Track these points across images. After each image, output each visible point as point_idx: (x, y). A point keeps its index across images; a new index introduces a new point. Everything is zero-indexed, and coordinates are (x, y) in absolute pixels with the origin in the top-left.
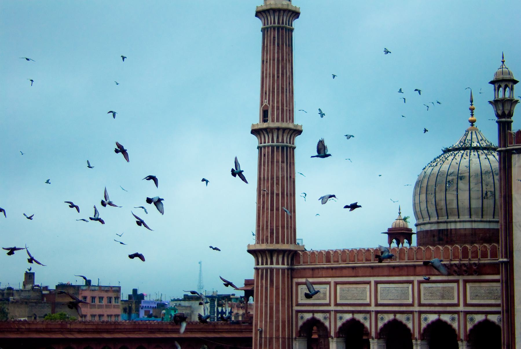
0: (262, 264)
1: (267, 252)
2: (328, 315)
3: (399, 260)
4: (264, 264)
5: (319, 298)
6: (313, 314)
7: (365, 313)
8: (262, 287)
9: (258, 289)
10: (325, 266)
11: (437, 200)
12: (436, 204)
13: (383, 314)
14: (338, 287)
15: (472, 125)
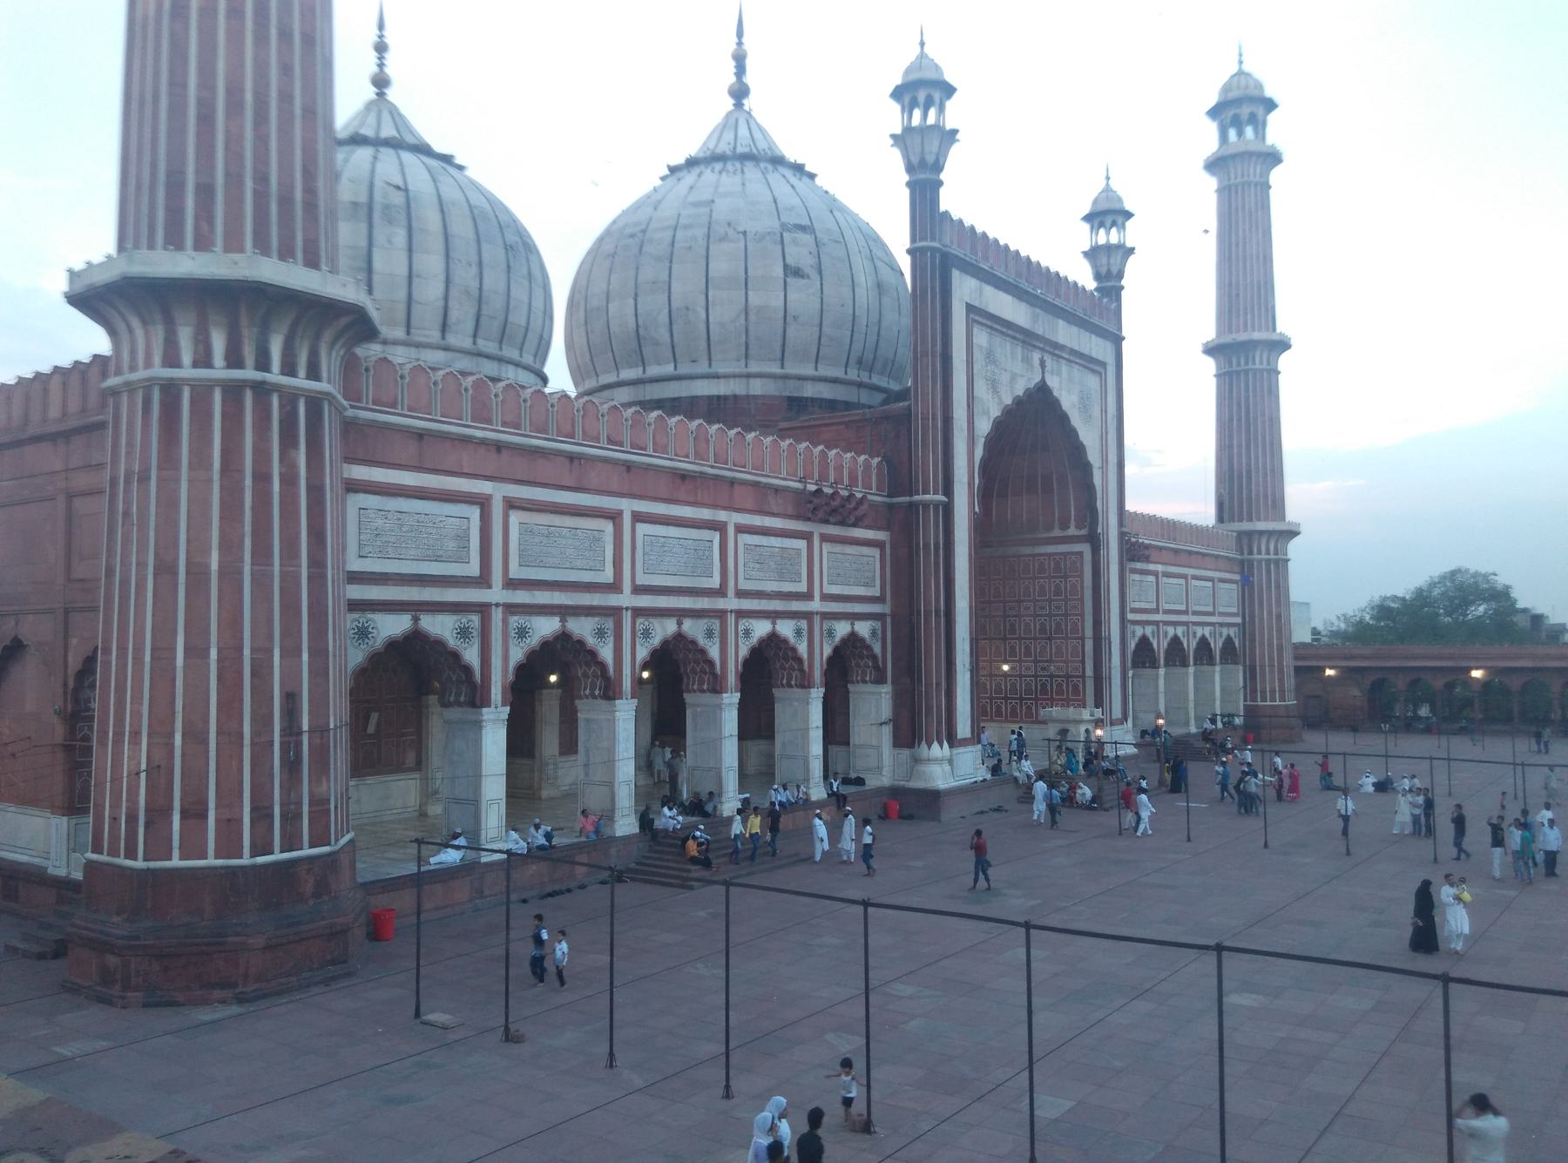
0: (289, 369)
1: (344, 321)
2: (475, 619)
3: (695, 459)
4: (302, 372)
5: (442, 556)
6: (416, 620)
7: (600, 615)
8: (289, 480)
9: (269, 494)
10: (479, 434)
11: (485, 287)
12: (483, 300)
13: (651, 620)
14: (515, 518)
15: (381, 95)
